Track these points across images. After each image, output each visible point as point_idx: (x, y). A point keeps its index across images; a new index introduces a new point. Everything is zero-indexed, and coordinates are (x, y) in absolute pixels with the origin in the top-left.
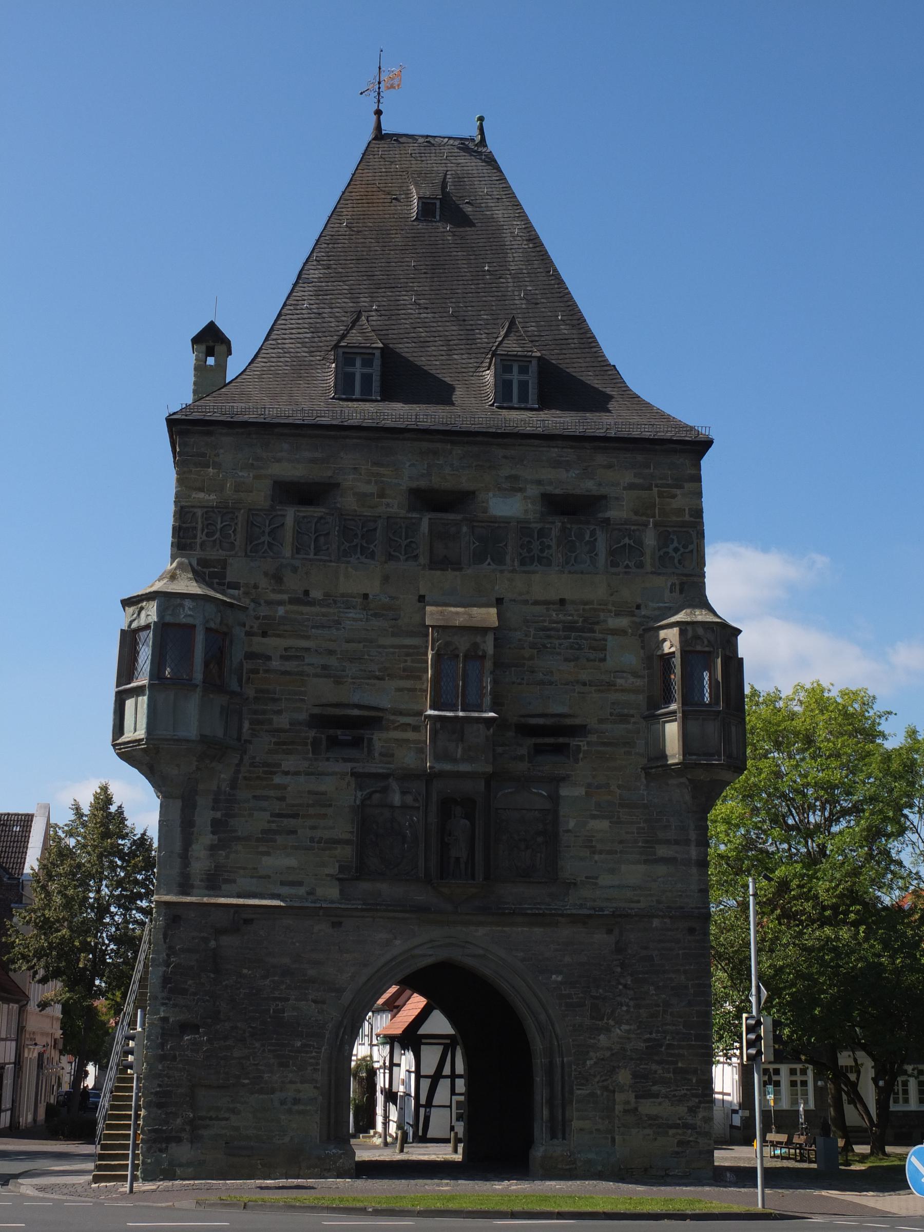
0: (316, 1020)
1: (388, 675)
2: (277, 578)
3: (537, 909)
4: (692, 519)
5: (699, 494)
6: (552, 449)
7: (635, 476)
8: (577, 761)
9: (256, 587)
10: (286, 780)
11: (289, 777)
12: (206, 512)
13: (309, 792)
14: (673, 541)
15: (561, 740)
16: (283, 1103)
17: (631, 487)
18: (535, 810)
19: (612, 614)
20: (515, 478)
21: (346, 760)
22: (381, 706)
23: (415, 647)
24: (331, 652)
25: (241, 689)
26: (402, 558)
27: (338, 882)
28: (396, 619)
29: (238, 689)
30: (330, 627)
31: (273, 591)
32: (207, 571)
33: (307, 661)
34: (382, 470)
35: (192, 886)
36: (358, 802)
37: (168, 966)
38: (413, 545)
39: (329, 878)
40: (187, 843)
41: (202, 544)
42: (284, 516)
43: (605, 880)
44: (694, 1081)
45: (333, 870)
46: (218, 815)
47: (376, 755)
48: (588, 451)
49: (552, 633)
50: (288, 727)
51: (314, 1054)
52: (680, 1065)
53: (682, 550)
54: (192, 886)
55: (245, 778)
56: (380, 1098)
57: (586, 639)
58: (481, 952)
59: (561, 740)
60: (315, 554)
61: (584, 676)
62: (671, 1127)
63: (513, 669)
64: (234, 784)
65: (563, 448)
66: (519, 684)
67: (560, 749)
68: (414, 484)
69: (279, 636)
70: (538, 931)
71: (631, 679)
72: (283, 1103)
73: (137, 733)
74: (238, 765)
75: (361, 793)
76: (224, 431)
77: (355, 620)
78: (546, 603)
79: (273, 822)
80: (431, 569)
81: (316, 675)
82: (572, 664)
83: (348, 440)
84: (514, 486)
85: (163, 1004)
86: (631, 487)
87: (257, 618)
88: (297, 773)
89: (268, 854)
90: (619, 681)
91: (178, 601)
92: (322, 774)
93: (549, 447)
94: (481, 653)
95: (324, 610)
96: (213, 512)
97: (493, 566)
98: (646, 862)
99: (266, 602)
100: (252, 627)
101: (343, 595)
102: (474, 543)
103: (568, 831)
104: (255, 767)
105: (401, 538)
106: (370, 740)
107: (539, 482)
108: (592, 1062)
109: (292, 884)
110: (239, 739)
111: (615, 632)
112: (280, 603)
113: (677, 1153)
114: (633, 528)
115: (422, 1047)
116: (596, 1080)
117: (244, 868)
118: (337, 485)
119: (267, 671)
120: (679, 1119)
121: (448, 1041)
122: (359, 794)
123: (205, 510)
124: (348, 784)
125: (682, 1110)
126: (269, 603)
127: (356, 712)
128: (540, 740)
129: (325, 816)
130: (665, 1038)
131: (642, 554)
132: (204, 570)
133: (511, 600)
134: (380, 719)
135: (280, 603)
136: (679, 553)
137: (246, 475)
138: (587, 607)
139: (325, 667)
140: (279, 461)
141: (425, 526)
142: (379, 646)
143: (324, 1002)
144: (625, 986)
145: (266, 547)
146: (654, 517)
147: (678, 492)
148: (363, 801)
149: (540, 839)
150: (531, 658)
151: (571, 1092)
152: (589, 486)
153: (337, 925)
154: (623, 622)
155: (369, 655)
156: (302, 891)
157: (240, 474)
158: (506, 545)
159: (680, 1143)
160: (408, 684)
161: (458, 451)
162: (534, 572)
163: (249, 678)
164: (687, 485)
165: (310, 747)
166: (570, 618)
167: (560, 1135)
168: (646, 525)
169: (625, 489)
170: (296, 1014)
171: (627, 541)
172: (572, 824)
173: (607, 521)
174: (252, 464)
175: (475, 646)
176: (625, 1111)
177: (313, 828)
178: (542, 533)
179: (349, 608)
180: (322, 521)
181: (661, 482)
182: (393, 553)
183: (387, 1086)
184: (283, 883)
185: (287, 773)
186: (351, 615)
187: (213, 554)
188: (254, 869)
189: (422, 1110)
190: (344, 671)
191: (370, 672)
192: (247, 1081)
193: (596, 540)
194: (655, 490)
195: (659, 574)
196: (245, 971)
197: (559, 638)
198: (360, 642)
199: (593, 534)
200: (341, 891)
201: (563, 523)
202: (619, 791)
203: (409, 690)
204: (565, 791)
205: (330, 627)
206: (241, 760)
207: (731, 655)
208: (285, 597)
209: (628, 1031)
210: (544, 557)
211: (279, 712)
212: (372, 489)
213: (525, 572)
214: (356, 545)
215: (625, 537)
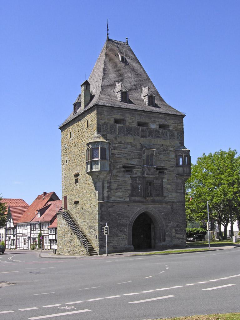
2: (116, 138)
9: (112, 140)
10: (120, 178)
13: (124, 180)
15: (163, 171)
16: (121, 239)
17: (173, 123)
20: (154, 121)
21: (129, 174)
23: (140, 153)
24: (126, 153)
31: (116, 141)
33: (122, 155)
35: (105, 199)
40: (103, 190)
43: (170, 196)
46: (108, 185)
47: (134, 173)
49: (161, 151)
54: (105, 199)
55: (113, 178)
59: (163, 171)
61: (166, 159)
69: (117, 150)
71: (173, 160)
72: (121, 239)
74: (111, 175)
78: (160, 145)
81: (123, 158)
84: (154, 122)
86: (173, 123)
87: (113, 146)
91: (104, 143)
92: (125, 177)
95: (124, 145)
98: (176, 193)
101: (127, 142)
106: (133, 170)
111: (171, 151)
112: (117, 143)
118: (125, 120)
119: (115, 157)
126: (115, 143)
127: (130, 165)
129: (126, 185)
131: (174, 136)
134: (134, 167)
135: (117, 143)
139: (125, 156)
147: (180, 125)
150: (158, 155)
154: (172, 149)
156: (123, 199)
159: (182, 241)
173: (169, 130)
176: (174, 236)
177: (124, 187)
185: (119, 177)
187: (105, 133)
199: (167, 132)
203: (139, 161)
208: (117, 142)
209: (174, 223)
211: (117, 165)
212: (131, 121)
213: (157, 139)
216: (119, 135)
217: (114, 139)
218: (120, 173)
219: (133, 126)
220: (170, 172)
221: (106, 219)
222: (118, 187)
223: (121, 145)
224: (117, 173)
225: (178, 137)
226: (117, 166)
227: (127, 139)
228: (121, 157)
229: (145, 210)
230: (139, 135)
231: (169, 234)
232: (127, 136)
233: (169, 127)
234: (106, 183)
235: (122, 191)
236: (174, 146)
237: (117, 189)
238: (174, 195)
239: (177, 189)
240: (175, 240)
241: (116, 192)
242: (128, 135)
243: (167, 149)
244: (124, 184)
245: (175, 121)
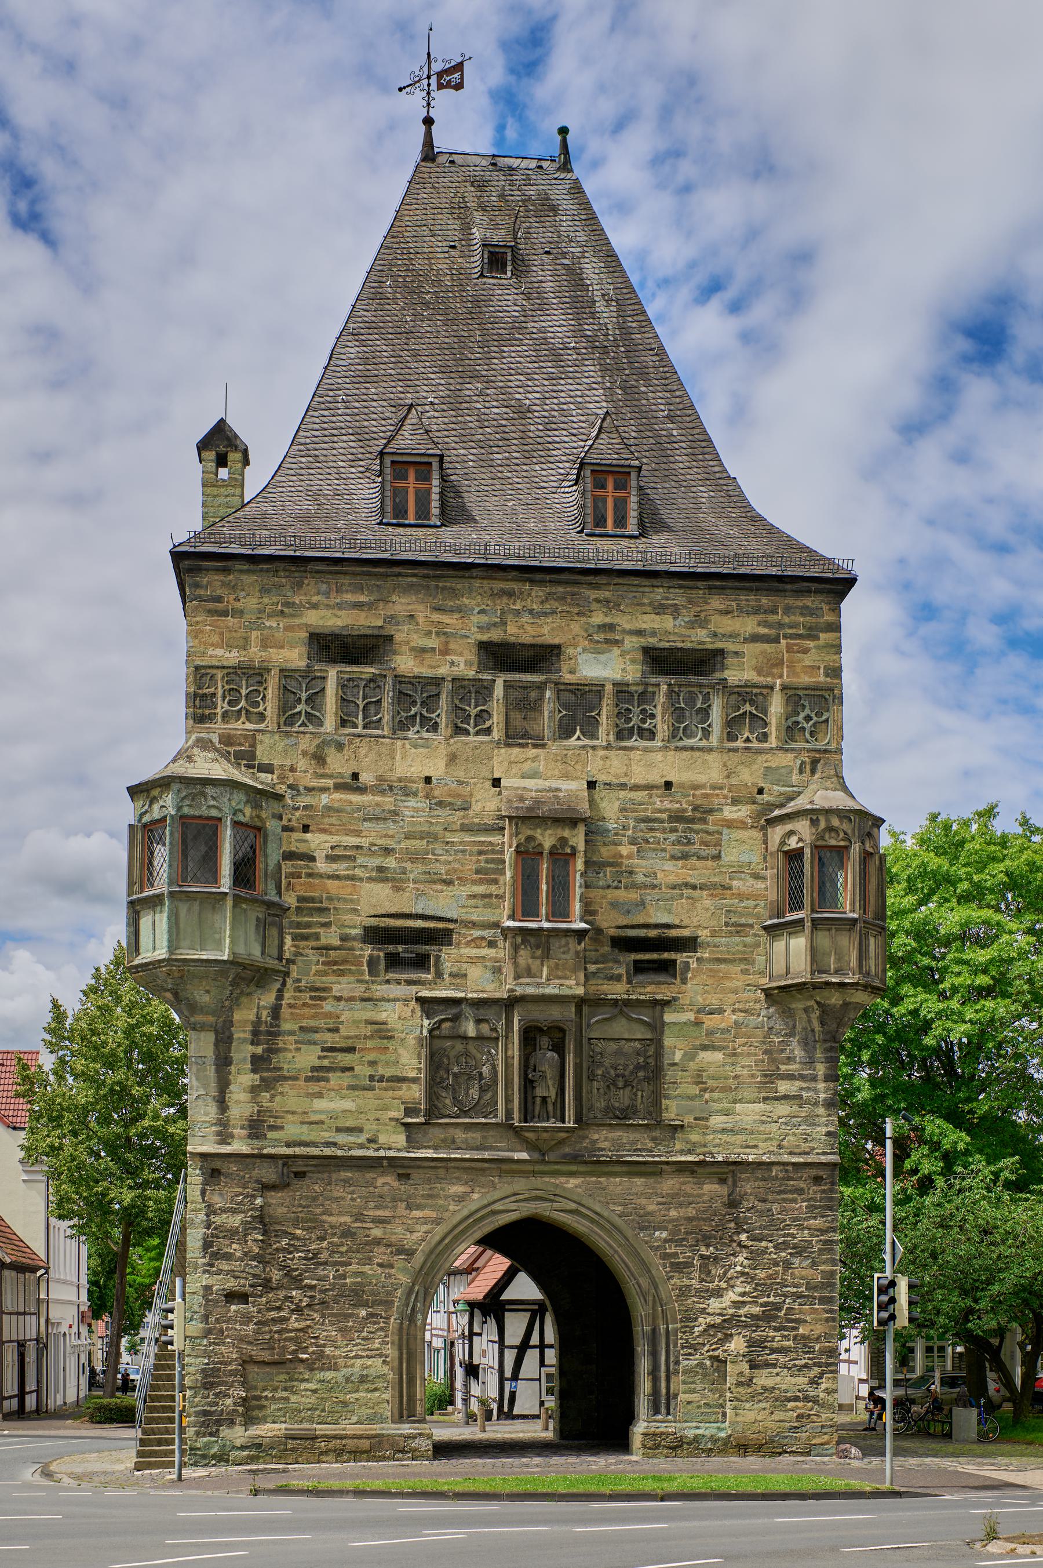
0: (383, 1287)
1: (458, 878)
2: (319, 758)
3: (638, 1156)
4: (828, 679)
5: (838, 648)
6: (656, 589)
7: (759, 625)
8: (684, 981)
9: (293, 769)
11: (342, 1003)
12: (228, 674)
14: (804, 706)
15: (666, 955)
17: (755, 638)
18: (635, 1040)
19: (729, 801)
20: (611, 627)
21: (409, 982)
22: (449, 916)
24: (388, 851)
25: (280, 897)
26: (471, 730)
27: (402, 1129)
28: (465, 809)
29: (277, 899)
30: (385, 819)
32: (231, 749)
33: (360, 860)
34: (445, 619)
35: (232, 1136)
36: (425, 1033)
37: (208, 1229)
38: (486, 715)
39: (393, 1123)
41: (225, 715)
42: (324, 678)
44: (817, 1349)
45: (399, 1114)
46: (259, 1050)
48: (701, 592)
50: (339, 943)
51: (382, 1325)
52: (801, 1331)
53: (815, 719)
55: (290, 1006)
56: (460, 1372)
57: (697, 832)
58: (573, 1206)
59: (666, 955)
60: (365, 727)
62: (789, 1400)
63: (608, 869)
64: (276, 1011)
65: (669, 587)
66: (616, 888)
67: (667, 968)
68: (484, 638)
69: (324, 831)
70: (639, 1181)
71: (751, 881)
73: (157, 952)
74: (280, 990)
75: (428, 1021)
76: (245, 567)
77: (415, 809)
78: (649, 787)
79: (325, 1057)
80: (507, 745)
81: (371, 879)
82: (680, 863)
83: (400, 579)
85: (205, 1272)
86: (755, 638)
88: (351, 999)
89: (320, 1095)
90: (735, 883)
93: (653, 586)
94: (569, 851)
95: (378, 799)
96: (236, 673)
97: (586, 742)
98: (766, 1099)
99: (306, 788)
100: (290, 820)
101: (400, 780)
102: (560, 712)
103: (675, 1064)
104: (300, 991)
105: (470, 706)
106: (438, 957)
107: (639, 633)
108: (701, 1328)
109: (350, 1130)
110: (280, 958)
111: (730, 824)
112: (324, 790)
113: (796, 1428)
114: (755, 691)
115: (506, 1313)
116: (706, 1348)
117: (293, 1113)
119: (310, 875)
120: (799, 1391)
121: (536, 1307)
122: (426, 1022)
123: (225, 671)
124: (413, 1011)
125: (802, 1380)
126: (309, 790)
127: (420, 924)
128: (640, 956)
130: (784, 1301)
131: (766, 724)
132: (229, 749)
133: (605, 784)
136: (811, 723)
137: (275, 625)
138: (698, 792)
139: (380, 869)
140: (315, 606)
141: (499, 691)
142: (448, 843)
143: (391, 1266)
144: (740, 1245)
145: (303, 718)
146: (781, 676)
147: (811, 644)
148: (430, 1032)
149: (641, 1074)
150: (629, 857)
151: (677, 1363)
152: (700, 638)
153: (404, 1177)
154: (743, 812)
155: (434, 854)
156: (362, 1139)
157: (268, 624)
158: (599, 714)
160: (480, 889)
161: (539, 592)
162: (632, 749)
163: (289, 883)
164: (822, 635)
165: (365, 968)
166: (678, 805)
167: (663, 1410)
168: (772, 688)
169: (746, 640)
170: (359, 1280)
171: (748, 707)
172: (678, 1056)
174: (282, 612)
175: (563, 841)
177: (373, 1063)
178: (646, 697)
179: (407, 795)
180: (372, 685)
181: (790, 631)
182: (461, 725)
183: (467, 1358)
184: (339, 1130)
185: (339, 999)
186: (409, 804)
188: (305, 1113)
189: (507, 1384)
190: (405, 873)
191: (435, 874)
192: (305, 1356)
193: (710, 706)
194: (783, 642)
195: (787, 750)
196: (298, 1232)
197: (664, 831)
198: (422, 838)
199: (706, 698)
200: (408, 1137)
201: (670, 685)
202: (734, 1017)
203: (484, 896)
204: (670, 1017)
205: (385, 819)
206: (284, 984)
207: (871, 850)
210: (645, 729)
211: (326, 925)
213: (621, 748)
214: (415, 716)
215: (745, 702)
216: (345, 740)
217: (302, 764)
218: (342, 973)
219: (443, 671)
220: (719, 960)
221: (238, 1254)
222: (326, 1063)
223: (356, 798)
224: (325, 973)
225: (792, 731)
226: (322, 931)
227: (398, 757)
228: (352, 878)
229: (529, 1209)
230: (488, 731)
231: (701, 1365)
232: (399, 743)
233: (723, 668)
234: (241, 1033)
235: (353, 1088)
236: (760, 791)
237: (318, 1074)
238: (749, 1112)
239: (771, 1077)
240: (748, 1405)
241: (316, 1089)
242: (410, 734)
243: (703, 813)
244: (370, 1044)
245: (772, 618)
